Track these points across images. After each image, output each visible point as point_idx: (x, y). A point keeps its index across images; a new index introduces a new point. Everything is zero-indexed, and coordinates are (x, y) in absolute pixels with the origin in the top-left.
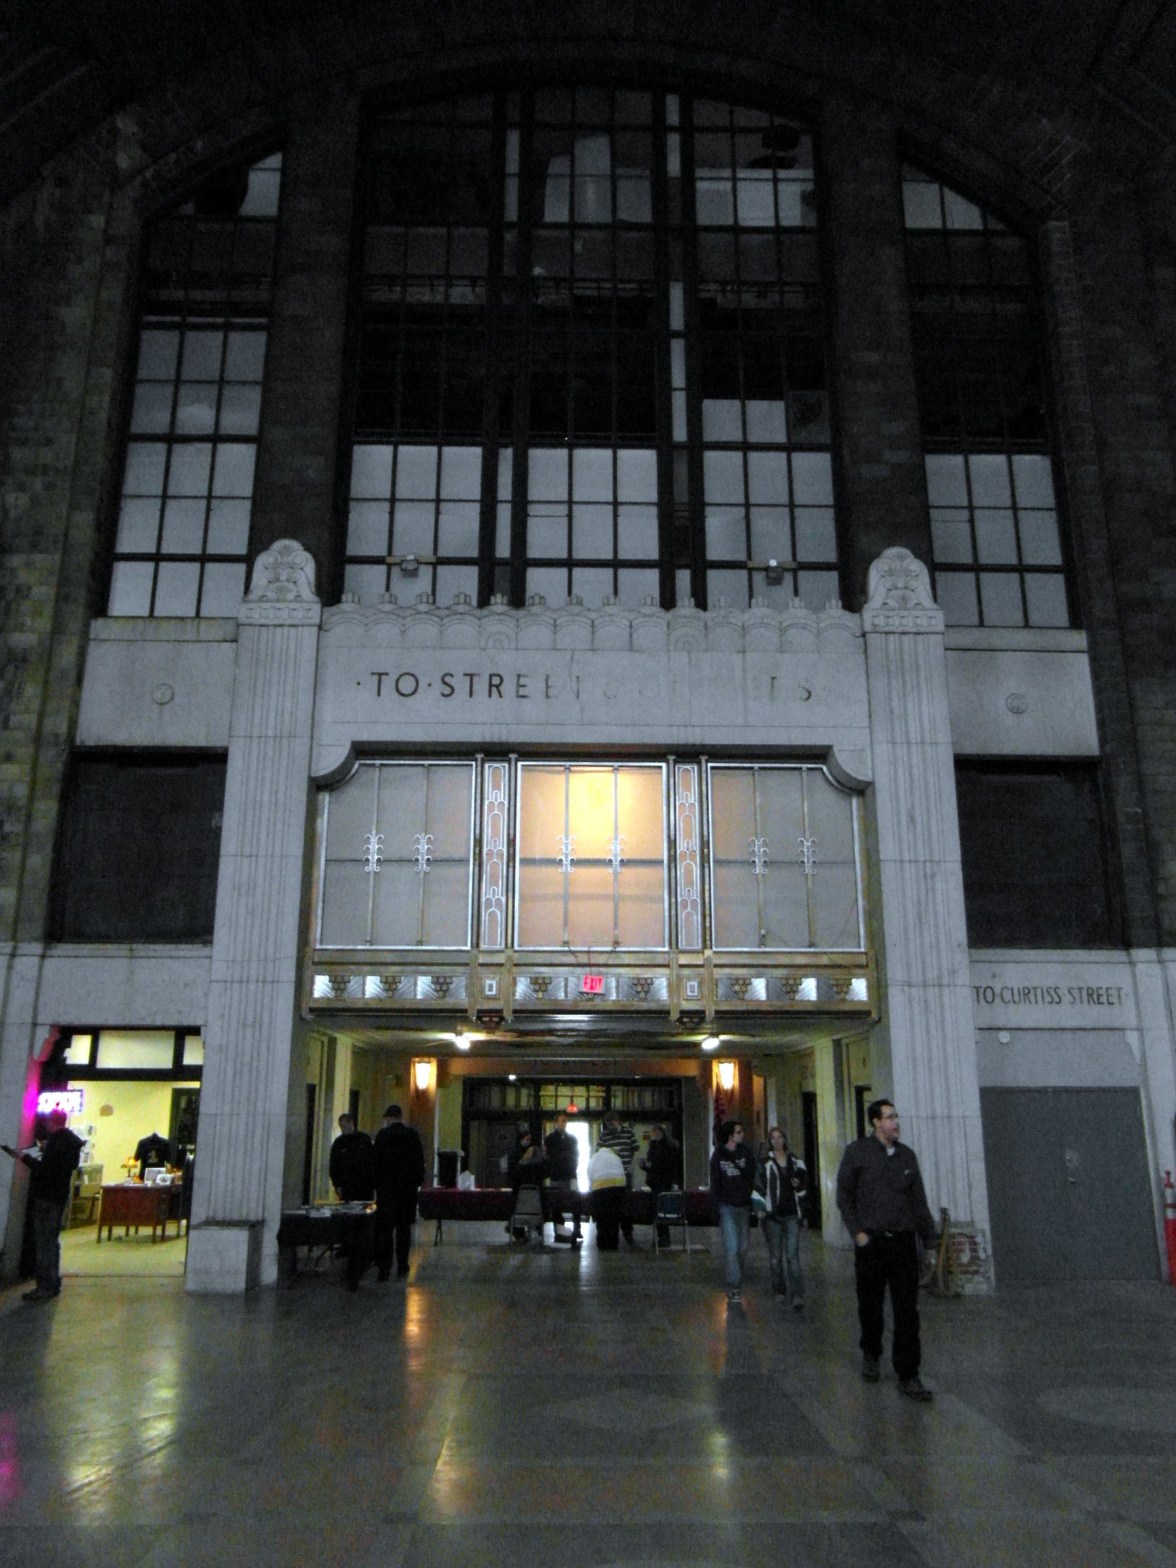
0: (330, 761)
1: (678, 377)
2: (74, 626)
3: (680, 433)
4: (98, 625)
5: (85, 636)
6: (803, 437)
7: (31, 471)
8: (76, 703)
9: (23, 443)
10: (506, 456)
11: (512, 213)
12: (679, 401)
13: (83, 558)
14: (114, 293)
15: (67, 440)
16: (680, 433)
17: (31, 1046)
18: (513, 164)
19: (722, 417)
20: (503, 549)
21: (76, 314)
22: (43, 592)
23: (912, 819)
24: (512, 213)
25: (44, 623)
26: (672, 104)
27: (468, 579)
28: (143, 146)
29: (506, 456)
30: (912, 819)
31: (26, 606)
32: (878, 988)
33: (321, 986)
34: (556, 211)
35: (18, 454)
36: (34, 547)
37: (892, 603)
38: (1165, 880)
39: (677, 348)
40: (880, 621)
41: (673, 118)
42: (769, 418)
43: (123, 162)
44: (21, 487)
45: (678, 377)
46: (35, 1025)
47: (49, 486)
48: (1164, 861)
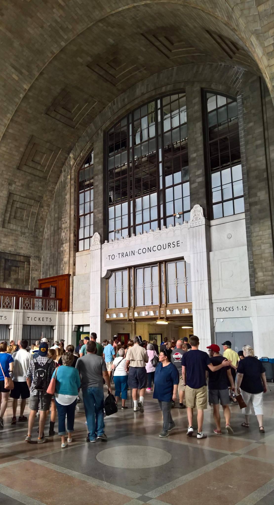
0: (104, 275)
1: (161, 174)
2: (72, 255)
3: (161, 187)
4: (77, 254)
5: (75, 256)
6: (185, 180)
7: (65, 229)
8: (74, 269)
9: (64, 223)
10: (132, 202)
11: (131, 146)
12: (161, 178)
13: (72, 243)
14: (73, 190)
15: (68, 221)
16: (161, 187)
17: (72, 329)
18: (131, 134)
19: (169, 179)
20: (132, 224)
21: (68, 197)
22: (68, 250)
23: (198, 271)
24: (131, 146)
25: (68, 256)
26: (159, 101)
27: (126, 232)
28: (74, 159)
29: (132, 202)
30: (198, 271)
31: (66, 253)
32: (190, 310)
33: (108, 316)
34: (138, 141)
35: (63, 226)
36: (66, 243)
37: (194, 220)
38: (257, 278)
39: (161, 165)
40: (191, 225)
41: (159, 106)
42: (178, 176)
43: (72, 163)
44: (64, 232)
45: (161, 174)
46: (72, 325)
47: (67, 231)
48: (257, 273)
